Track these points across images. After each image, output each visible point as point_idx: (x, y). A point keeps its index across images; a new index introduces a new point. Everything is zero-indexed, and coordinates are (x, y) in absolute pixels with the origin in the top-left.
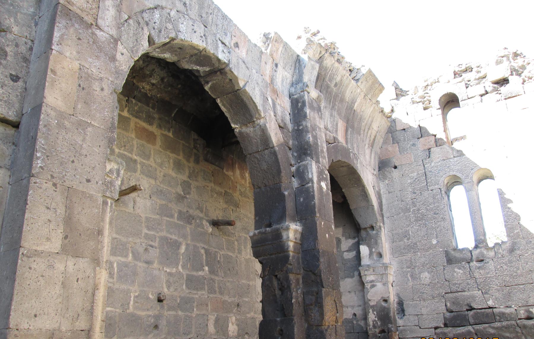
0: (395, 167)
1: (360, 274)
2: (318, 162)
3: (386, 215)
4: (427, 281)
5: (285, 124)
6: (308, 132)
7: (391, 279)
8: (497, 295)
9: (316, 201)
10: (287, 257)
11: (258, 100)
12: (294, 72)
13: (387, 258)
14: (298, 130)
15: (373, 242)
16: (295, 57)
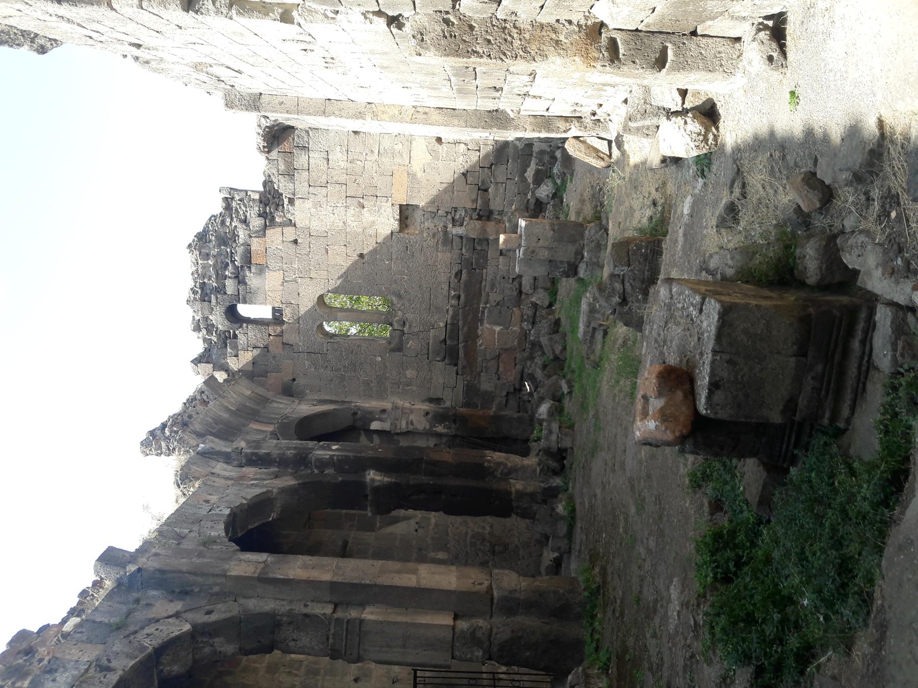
0: (294, 380)
1: (398, 434)
2: (313, 449)
3: (342, 398)
4: (414, 373)
5: (273, 473)
6: (284, 454)
7: (407, 405)
8: (436, 317)
9: (351, 454)
10: (395, 483)
11: (258, 491)
12: (214, 459)
13: (387, 405)
14: (279, 463)
15: (369, 416)
16: (198, 456)
